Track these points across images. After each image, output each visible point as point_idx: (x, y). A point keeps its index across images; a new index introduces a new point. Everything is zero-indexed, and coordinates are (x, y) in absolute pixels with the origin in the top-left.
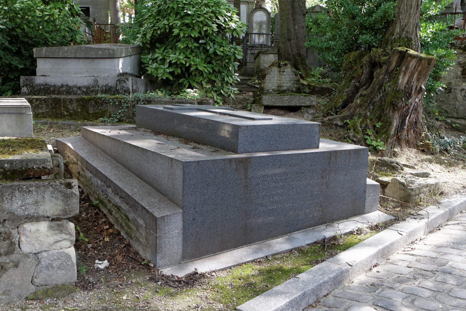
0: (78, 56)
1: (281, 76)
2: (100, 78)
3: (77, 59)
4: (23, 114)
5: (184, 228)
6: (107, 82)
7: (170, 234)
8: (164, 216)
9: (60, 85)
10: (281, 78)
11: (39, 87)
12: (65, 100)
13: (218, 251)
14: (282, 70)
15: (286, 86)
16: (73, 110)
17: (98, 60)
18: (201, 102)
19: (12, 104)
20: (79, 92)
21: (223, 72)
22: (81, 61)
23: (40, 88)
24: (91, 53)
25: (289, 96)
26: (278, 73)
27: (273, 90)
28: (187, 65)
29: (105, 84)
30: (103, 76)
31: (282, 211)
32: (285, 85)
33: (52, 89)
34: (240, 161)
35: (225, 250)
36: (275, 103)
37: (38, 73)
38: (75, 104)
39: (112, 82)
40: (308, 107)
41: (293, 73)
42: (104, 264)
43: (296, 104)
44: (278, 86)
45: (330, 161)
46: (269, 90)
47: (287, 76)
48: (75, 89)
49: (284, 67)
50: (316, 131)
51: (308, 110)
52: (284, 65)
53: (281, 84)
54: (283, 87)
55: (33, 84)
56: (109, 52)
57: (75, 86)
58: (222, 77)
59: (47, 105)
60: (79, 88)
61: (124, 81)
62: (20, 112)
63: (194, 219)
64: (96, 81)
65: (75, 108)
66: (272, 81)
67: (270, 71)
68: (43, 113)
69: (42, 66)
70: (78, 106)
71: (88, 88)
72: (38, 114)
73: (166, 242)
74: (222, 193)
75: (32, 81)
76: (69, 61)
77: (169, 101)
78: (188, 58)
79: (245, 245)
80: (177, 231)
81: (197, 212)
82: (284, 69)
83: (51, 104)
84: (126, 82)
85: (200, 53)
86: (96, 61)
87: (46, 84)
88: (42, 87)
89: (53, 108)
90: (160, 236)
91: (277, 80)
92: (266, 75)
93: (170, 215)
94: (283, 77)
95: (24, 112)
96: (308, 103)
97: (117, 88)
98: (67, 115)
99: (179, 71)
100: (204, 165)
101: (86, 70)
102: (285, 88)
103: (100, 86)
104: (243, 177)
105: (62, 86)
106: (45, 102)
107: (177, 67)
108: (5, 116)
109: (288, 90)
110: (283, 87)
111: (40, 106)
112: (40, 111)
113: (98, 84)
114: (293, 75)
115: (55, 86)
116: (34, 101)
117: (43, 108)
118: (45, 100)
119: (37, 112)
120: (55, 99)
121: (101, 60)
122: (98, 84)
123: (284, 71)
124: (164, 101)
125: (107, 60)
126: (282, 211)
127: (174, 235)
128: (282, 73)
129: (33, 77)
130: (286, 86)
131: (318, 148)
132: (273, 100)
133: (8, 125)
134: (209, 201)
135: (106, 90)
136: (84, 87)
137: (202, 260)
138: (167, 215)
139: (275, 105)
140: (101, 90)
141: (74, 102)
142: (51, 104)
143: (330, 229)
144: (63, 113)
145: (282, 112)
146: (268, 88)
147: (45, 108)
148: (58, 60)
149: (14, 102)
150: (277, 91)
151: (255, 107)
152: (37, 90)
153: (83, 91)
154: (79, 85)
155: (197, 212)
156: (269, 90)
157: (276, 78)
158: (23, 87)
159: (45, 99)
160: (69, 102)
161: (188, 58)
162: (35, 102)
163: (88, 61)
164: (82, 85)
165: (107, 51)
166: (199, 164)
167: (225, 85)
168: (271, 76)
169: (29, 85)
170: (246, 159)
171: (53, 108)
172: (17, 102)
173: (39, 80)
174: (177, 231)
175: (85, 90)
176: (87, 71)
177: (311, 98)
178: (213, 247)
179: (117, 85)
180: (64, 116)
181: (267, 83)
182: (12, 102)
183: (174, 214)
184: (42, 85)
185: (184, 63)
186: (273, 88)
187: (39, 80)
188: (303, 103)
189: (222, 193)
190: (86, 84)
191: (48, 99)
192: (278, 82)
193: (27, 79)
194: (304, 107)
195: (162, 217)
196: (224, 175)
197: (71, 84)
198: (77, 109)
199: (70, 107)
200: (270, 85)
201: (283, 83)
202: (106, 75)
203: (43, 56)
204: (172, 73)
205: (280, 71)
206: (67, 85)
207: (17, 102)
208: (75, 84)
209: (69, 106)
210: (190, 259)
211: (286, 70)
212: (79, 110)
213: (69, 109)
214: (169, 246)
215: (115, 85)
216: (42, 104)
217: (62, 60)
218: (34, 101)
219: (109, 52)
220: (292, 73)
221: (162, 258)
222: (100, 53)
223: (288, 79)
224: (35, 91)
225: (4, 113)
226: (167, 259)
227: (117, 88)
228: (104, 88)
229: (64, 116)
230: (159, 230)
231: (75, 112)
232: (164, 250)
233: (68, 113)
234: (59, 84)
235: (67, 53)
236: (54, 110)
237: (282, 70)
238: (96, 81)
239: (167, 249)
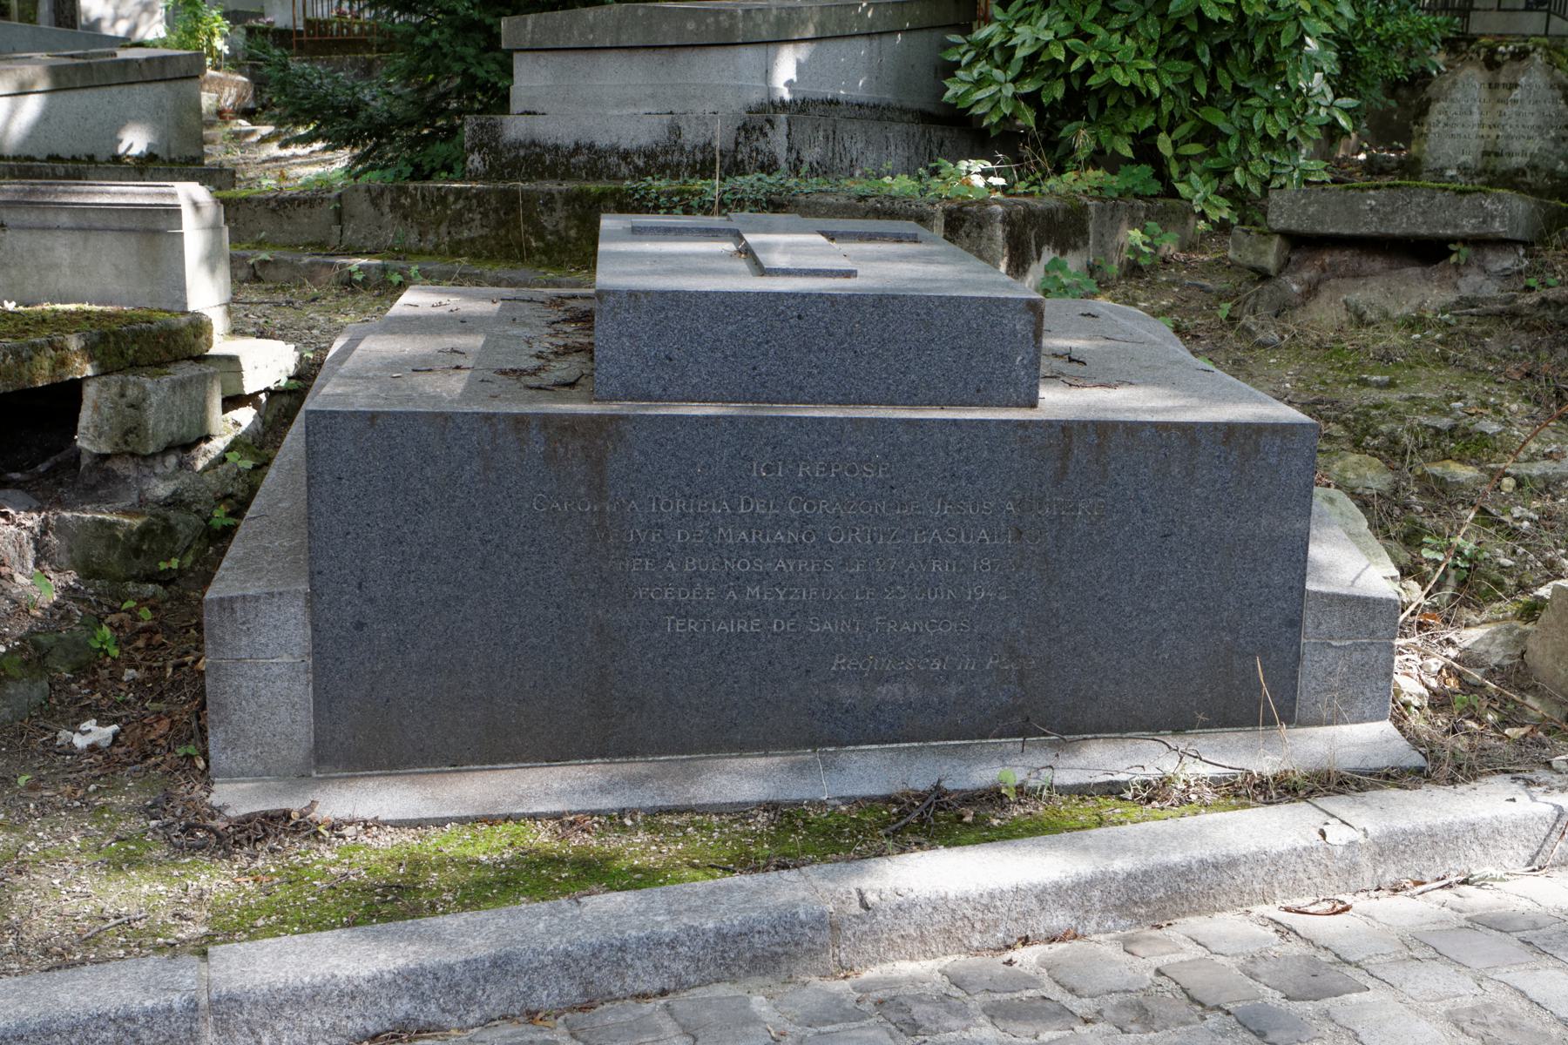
0: (625, 40)
1: (1500, 107)
2: (688, 121)
3: (625, 53)
4: (157, 232)
5: (318, 650)
6: (709, 135)
7: (256, 665)
8: (232, 600)
9: (572, 146)
10: (1501, 114)
11: (513, 154)
12: (529, 197)
13: (473, 761)
14: (1502, 80)
15: (1524, 154)
16: (557, 233)
17: (688, 52)
18: (960, 209)
19: (116, 201)
20: (624, 170)
21: (1254, 95)
22: (638, 57)
23: (517, 156)
24: (665, 27)
25: (1384, 192)
26: (1485, 94)
27: (1463, 169)
28: (1076, 65)
29: (701, 141)
30: (699, 111)
31: (790, 648)
32: (1516, 146)
33: (548, 159)
34: (565, 429)
35: (503, 761)
36: (1322, 223)
37: (515, 106)
38: (560, 213)
39: (721, 136)
40: (1481, 242)
41: (1558, 93)
42: (95, 733)
43: (1412, 230)
44: (1486, 153)
45: (1064, 469)
46: (1442, 170)
47: (1530, 108)
48: (613, 160)
49: (1516, 66)
50: (1014, 333)
51: (1490, 256)
52: (1513, 54)
53: (1502, 143)
54: (1510, 155)
55: (496, 140)
56: (717, 22)
57: (614, 150)
58: (1246, 113)
59: (485, 215)
60: (625, 156)
61: (761, 129)
62: (152, 226)
63: (360, 626)
64: (675, 130)
65: (561, 226)
66: (1458, 130)
67: (1446, 85)
68: (472, 240)
69: (531, 79)
70: (568, 218)
71: (650, 155)
72: (459, 242)
73: (244, 691)
74: (484, 542)
75: (494, 131)
76: (603, 58)
77: (846, 206)
78: (1087, 37)
79: (602, 756)
80: (286, 659)
81: (371, 600)
82: (1515, 73)
83: (496, 211)
84: (766, 135)
85: (1144, 17)
86: (683, 57)
87: (533, 143)
88: (522, 153)
89: (501, 224)
90: (218, 668)
91: (1481, 125)
92: (1429, 101)
93: (257, 598)
94: (1510, 110)
95: (162, 225)
96: (1468, 226)
97: (739, 157)
98: (537, 249)
99: (1059, 92)
100: (395, 431)
101: (649, 91)
102: (1518, 161)
103: (688, 148)
104: (582, 490)
105: (578, 148)
106: (479, 205)
107: (1053, 77)
108: (109, 237)
109: (1535, 168)
110: (1510, 155)
111: (468, 216)
112: (466, 234)
113: (681, 141)
114: (1554, 101)
115: (557, 147)
116: (451, 198)
117: (473, 224)
118: (479, 195)
119: (457, 237)
120: (505, 192)
121: (696, 50)
122: (681, 141)
123: (1516, 85)
124: (829, 205)
125: (715, 55)
126: (790, 648)
127: (276, 670)
128: (1502, 93)
129: (498, 117)
130: (1524, 154)
131: (1033, 404)
132: (1311, 210)
133: (116, 266)
134: (424, 568)
135: (703, 162)
136: (640, 151)
137: (391, 780)
138: (244, 597)
139: (1319, 229)
140: (688, 165)
141: (559, 206)
142: (496, 211)
143: (1066, 760)
144: (528, 241)
145: (1378, 264)
146: (1441, 162)
147: (477, 222)
148: (572, 56)
149: (139, 194)
150: (1479, 175)
151: (1242, 236)
152: (508, 165)
153: (636, 167)
154: (625, 144)
155: (371, 600)
156: (1442, 170)
157: (1476, 117)
158: (472, 151)
159: (480, 191)
160: (545, 204)
161: (1087, 37)
162: (455, 202)
163: (656, 56)
164: (635, 145)
165: (711, 20)
166: (372, 425)
167: (1254, 148)
168: (1455, 108)
169: (486, 145)
170: (597, 421)
171: (501, 224)
172: (148, 194)
173: (514, 128)
174: (286, 659)
175: (641, 163)
176: (653, 96)
177: (1487, 204)
178: (452, 740)
179: (737, 144)
180: (530, 253)
181: (1433, 139)
182: (134, 194)
183: (272, 595)
184: (522, 145)
185: (1061, 57)
186: (1463, 158)
187: (514, 128)
188: (1446, 225)
189: (484, 542)
190: (645, 140)
191: (488, 191)
192: (1484, 131)
193: (482, 126)
194: (1466, 241)
195: (222, 599)
196: (492, 475)
197: (602, 141)
198: (567, 228)
199: (547, 221)
200: (1449, 146)
201: (1509, 137)
202: (710, 107)
203: (527, 46)
204: (1032, 99)
205: (1493, 86)
206: (591, 147)
207: (148, 194)
208: (615, 140)
209: (543, 218)
210: (346, 769)
211: (1523, 80)
212: (573, 233)
213: (544, 228)
214: (255, 707)
215: (732, 146)
216: (470, 210)
217: (582, 56)
218: (451, 198)
219: (717, 22)
220: (1549, 94)
221: (231, 744)
222: (691, 26)
223: (1532, 121)
224: (503, 166)
225: (105, 229)
226: (252, 751)
227: (739, 157)
228: (699, 157)
229: (530, 253)
230: (215, 643)
231: (561, 238)
232: (235, 718)
233: (541, 244)
234: (568, 142)
235: (592, 31)
236: (502, 232)
237: (1502, 80)
238: (675, 130)
239: (247, 717)
